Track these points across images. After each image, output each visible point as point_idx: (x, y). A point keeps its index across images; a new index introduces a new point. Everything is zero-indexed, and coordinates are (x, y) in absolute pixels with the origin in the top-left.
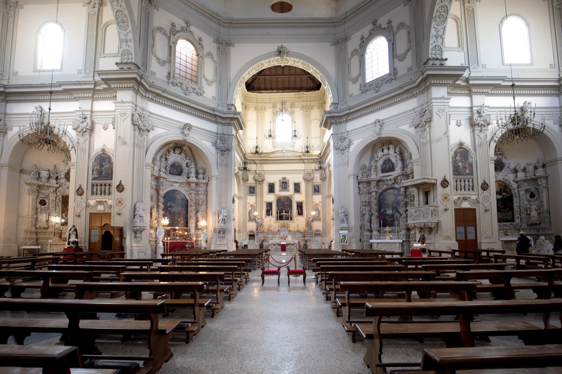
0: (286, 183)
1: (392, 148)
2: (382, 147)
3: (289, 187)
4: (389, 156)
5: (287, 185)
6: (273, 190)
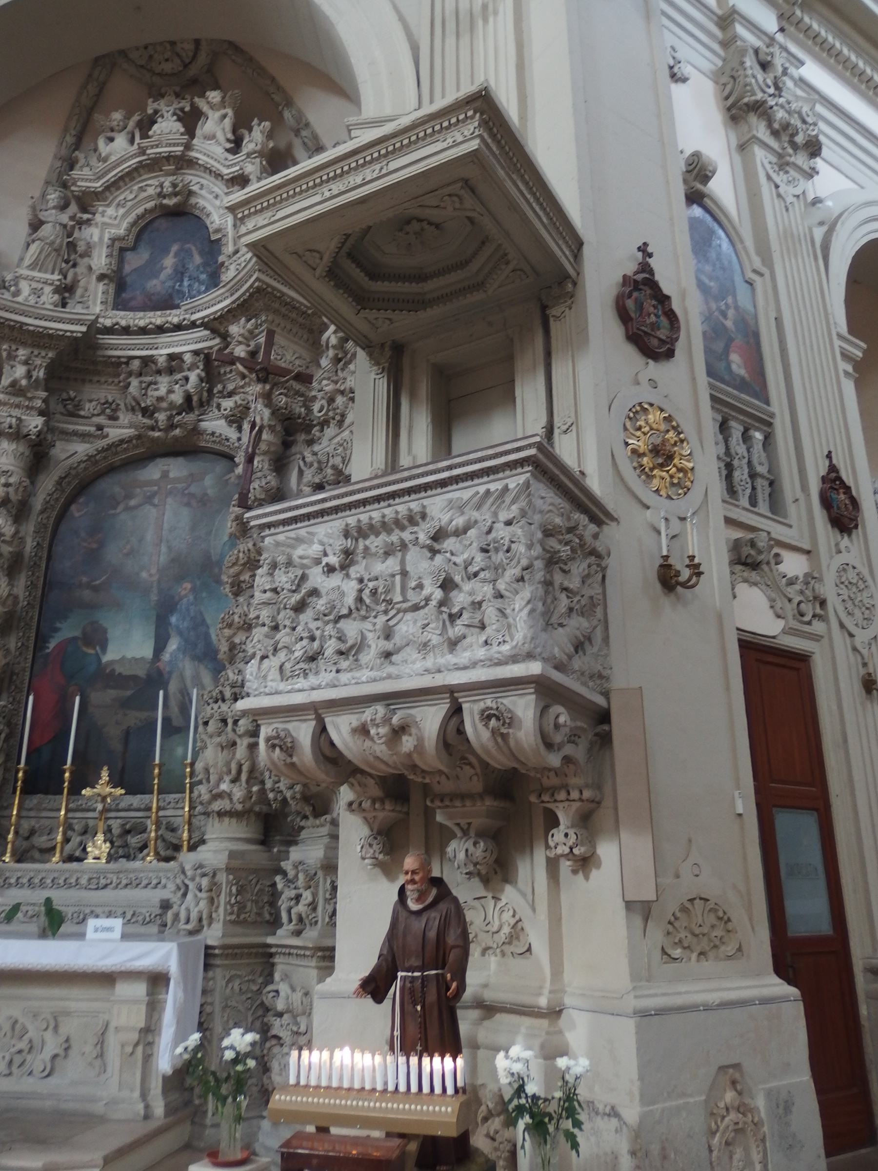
1: (214, 116)
2: (144, 110)
4: (193, 179)
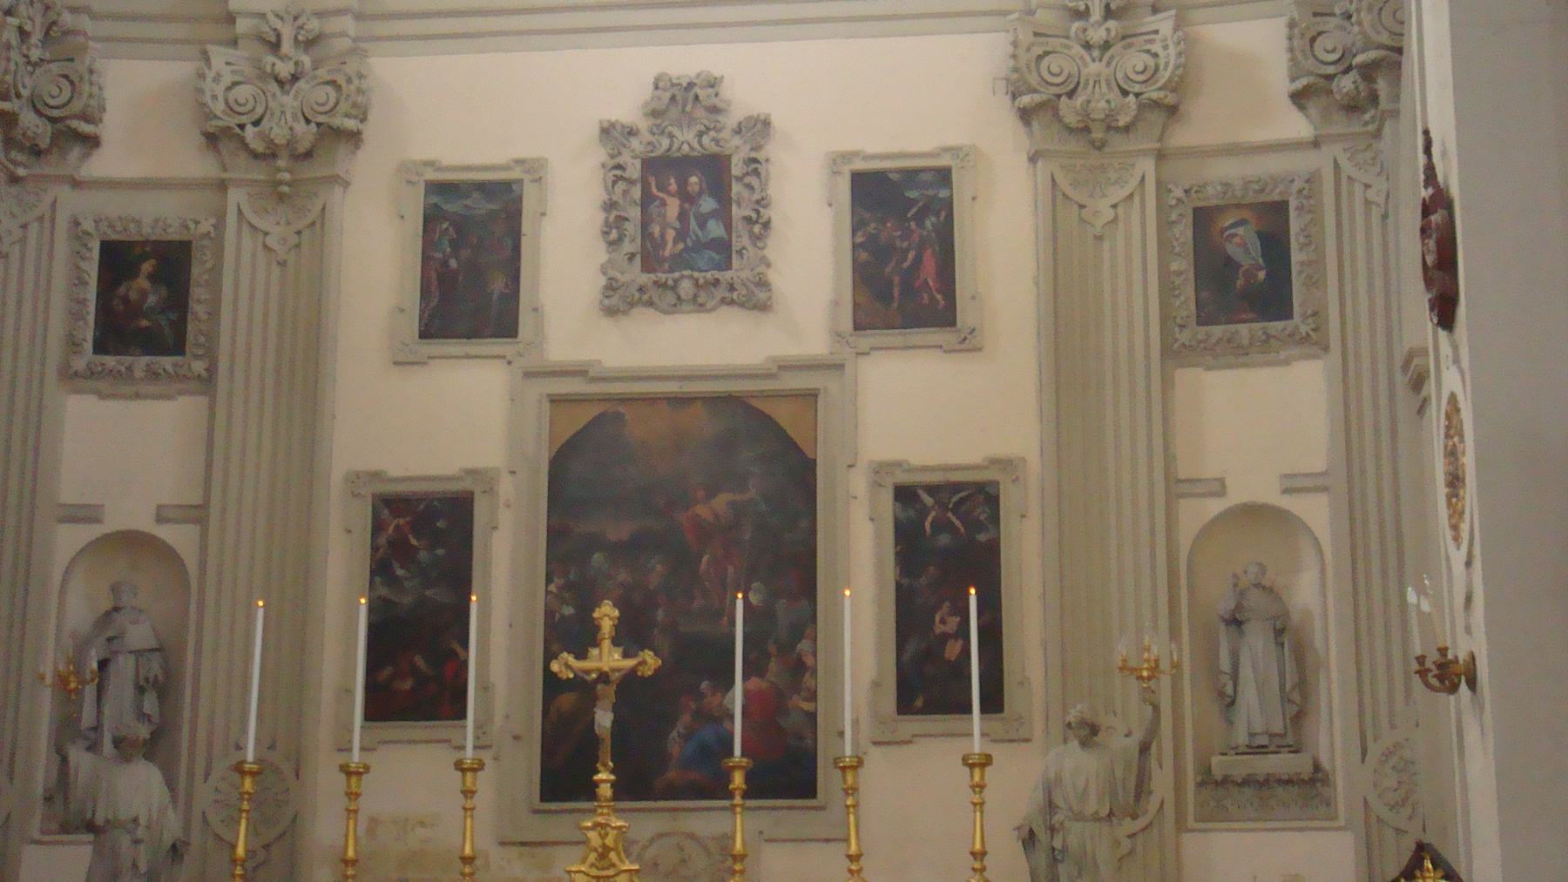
0: (715, 169)
3: (774, 249)
5: (736, 212)
6: (498, 285)
